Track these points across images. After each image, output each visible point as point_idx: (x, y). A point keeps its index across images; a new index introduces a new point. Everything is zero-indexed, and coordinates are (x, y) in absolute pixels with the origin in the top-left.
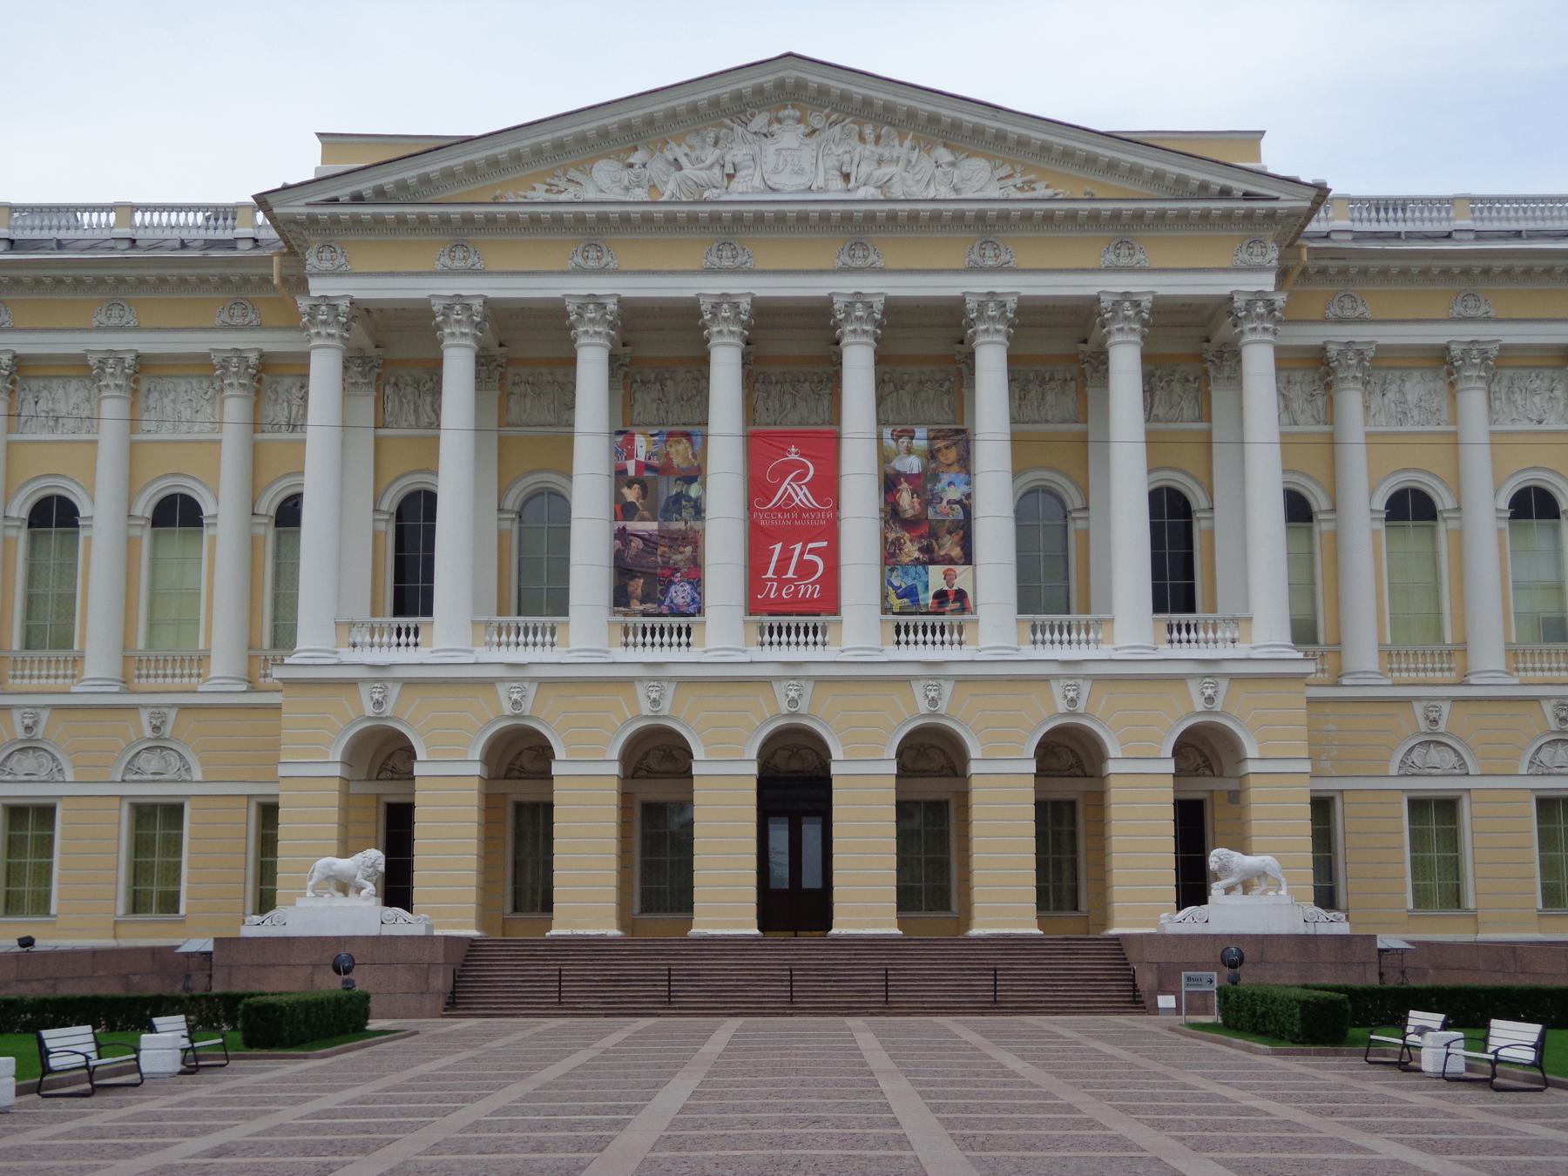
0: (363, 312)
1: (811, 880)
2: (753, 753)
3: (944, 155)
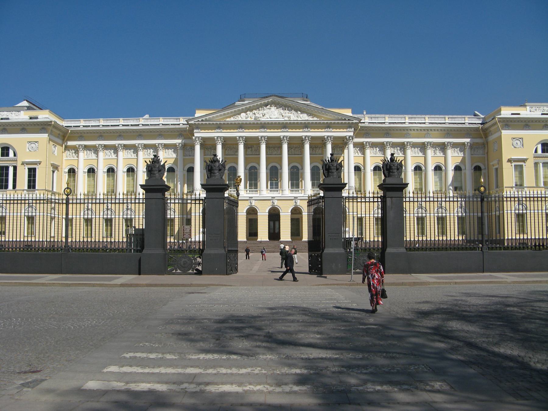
0: (203, 138)
1: (277, 231)
2: (267, 211)
3: (299, 112)
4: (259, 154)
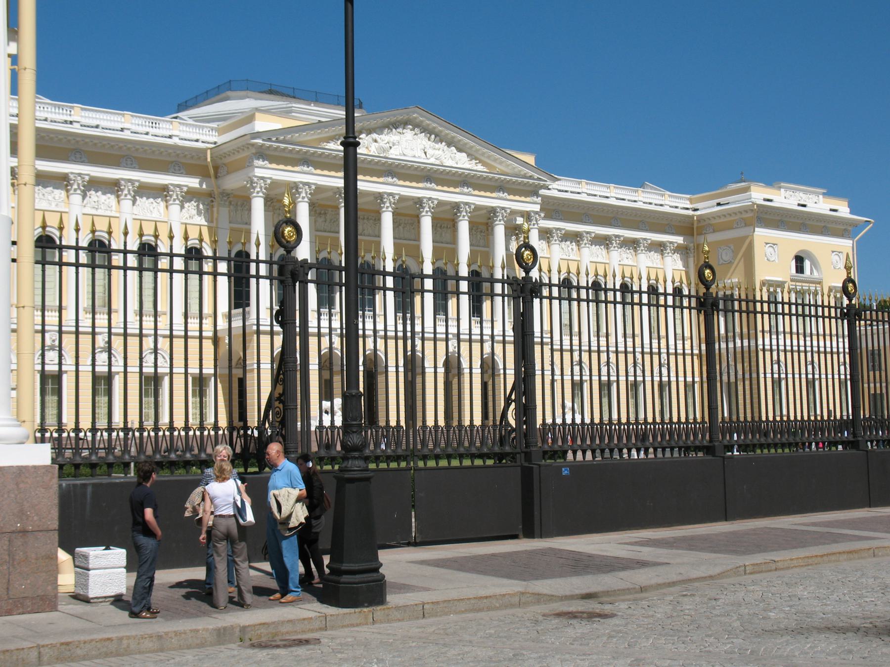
4: (379, 236)
